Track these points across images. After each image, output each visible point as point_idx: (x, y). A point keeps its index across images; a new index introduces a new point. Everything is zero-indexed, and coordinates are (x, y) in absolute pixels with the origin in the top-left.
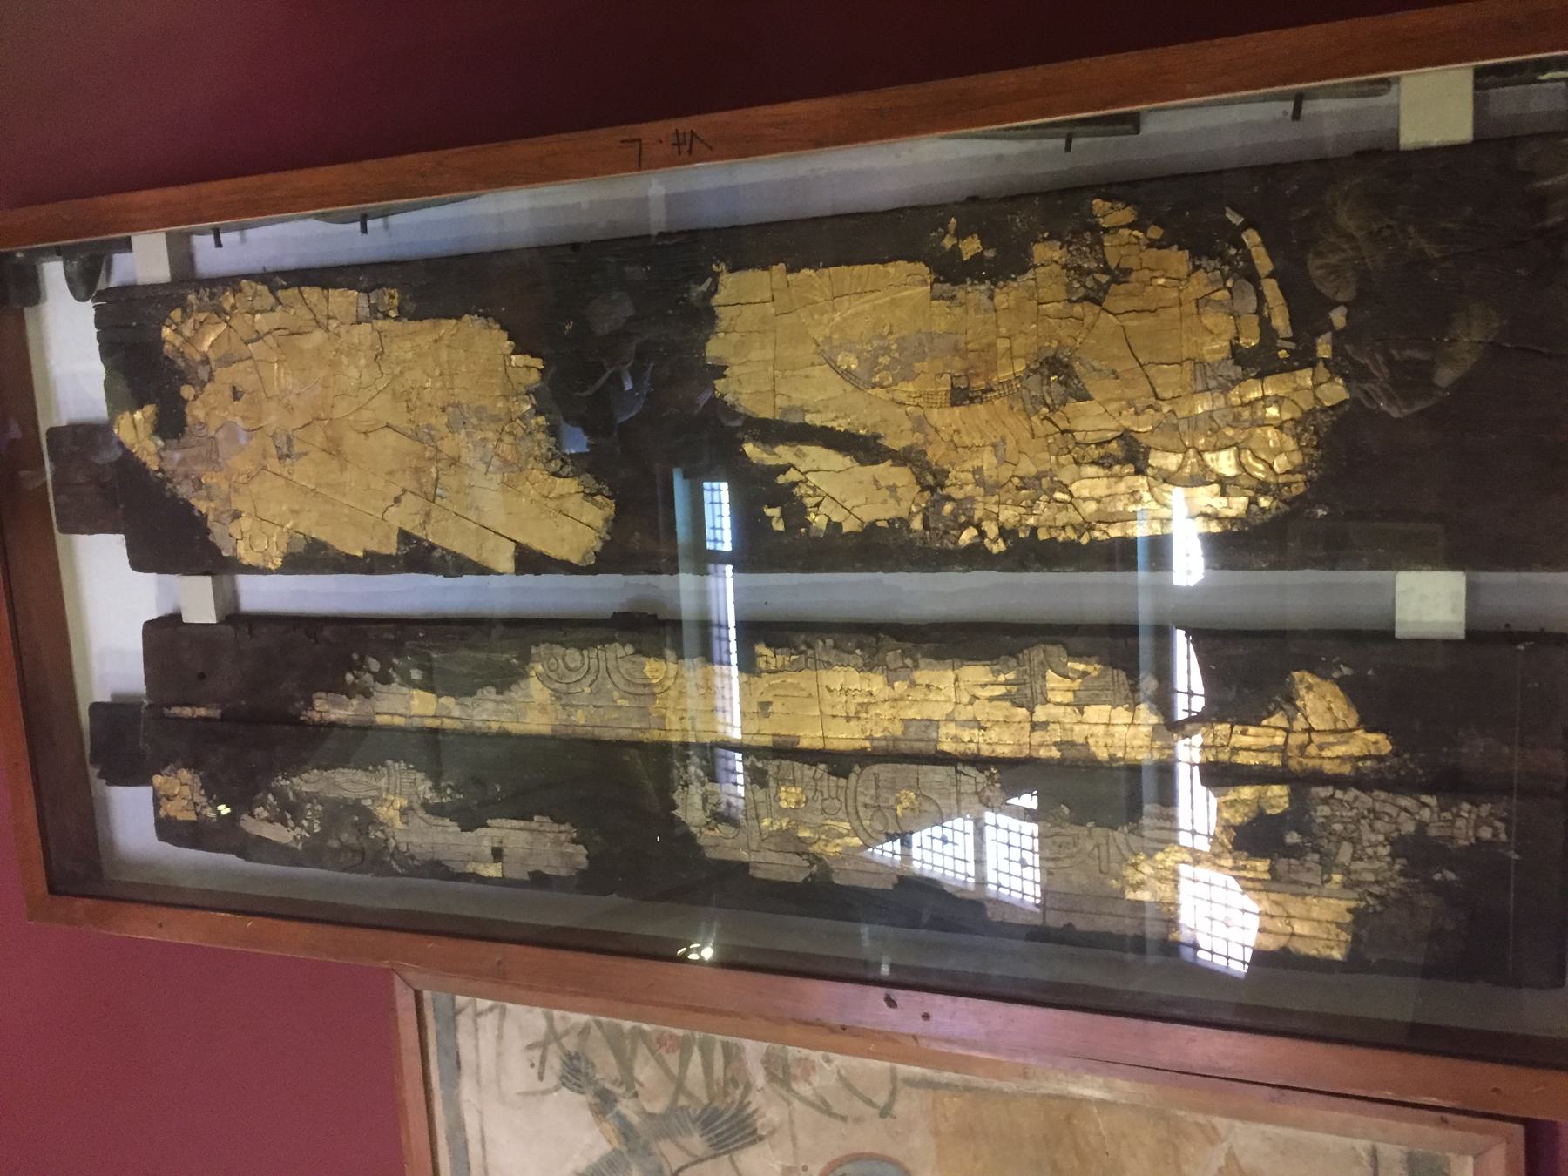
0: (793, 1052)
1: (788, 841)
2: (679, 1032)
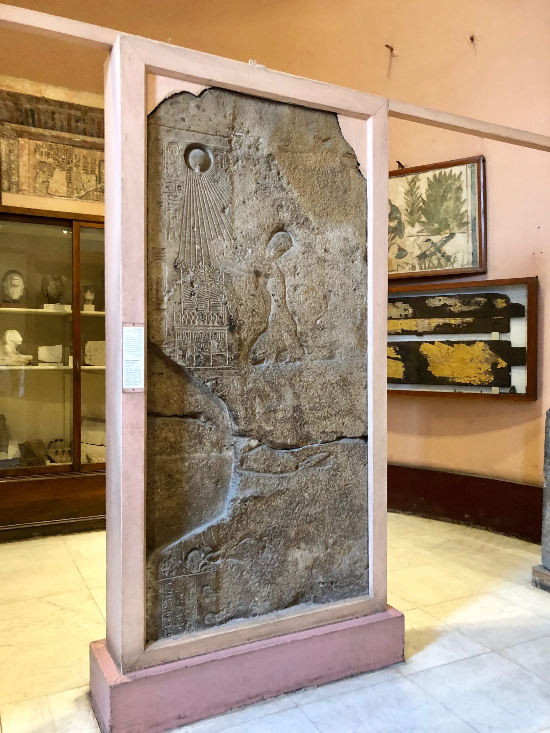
0: (411, 271)
1: (398, 307)
2: (430, 270)
